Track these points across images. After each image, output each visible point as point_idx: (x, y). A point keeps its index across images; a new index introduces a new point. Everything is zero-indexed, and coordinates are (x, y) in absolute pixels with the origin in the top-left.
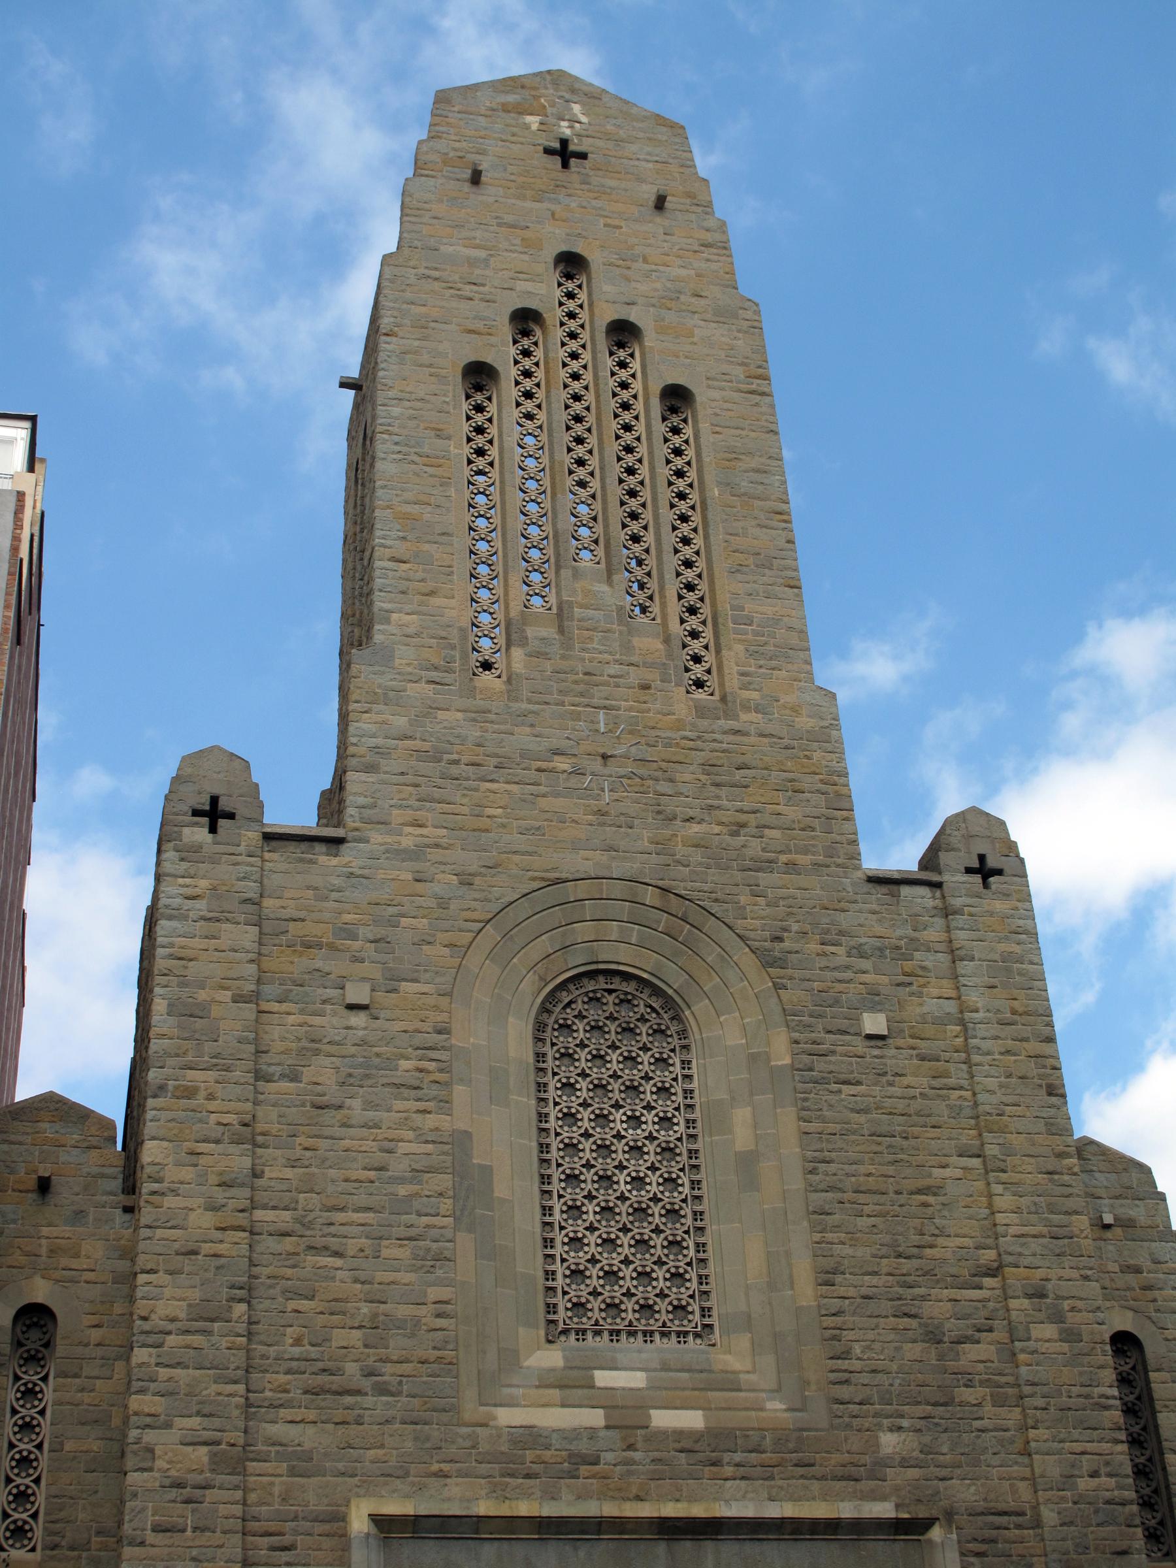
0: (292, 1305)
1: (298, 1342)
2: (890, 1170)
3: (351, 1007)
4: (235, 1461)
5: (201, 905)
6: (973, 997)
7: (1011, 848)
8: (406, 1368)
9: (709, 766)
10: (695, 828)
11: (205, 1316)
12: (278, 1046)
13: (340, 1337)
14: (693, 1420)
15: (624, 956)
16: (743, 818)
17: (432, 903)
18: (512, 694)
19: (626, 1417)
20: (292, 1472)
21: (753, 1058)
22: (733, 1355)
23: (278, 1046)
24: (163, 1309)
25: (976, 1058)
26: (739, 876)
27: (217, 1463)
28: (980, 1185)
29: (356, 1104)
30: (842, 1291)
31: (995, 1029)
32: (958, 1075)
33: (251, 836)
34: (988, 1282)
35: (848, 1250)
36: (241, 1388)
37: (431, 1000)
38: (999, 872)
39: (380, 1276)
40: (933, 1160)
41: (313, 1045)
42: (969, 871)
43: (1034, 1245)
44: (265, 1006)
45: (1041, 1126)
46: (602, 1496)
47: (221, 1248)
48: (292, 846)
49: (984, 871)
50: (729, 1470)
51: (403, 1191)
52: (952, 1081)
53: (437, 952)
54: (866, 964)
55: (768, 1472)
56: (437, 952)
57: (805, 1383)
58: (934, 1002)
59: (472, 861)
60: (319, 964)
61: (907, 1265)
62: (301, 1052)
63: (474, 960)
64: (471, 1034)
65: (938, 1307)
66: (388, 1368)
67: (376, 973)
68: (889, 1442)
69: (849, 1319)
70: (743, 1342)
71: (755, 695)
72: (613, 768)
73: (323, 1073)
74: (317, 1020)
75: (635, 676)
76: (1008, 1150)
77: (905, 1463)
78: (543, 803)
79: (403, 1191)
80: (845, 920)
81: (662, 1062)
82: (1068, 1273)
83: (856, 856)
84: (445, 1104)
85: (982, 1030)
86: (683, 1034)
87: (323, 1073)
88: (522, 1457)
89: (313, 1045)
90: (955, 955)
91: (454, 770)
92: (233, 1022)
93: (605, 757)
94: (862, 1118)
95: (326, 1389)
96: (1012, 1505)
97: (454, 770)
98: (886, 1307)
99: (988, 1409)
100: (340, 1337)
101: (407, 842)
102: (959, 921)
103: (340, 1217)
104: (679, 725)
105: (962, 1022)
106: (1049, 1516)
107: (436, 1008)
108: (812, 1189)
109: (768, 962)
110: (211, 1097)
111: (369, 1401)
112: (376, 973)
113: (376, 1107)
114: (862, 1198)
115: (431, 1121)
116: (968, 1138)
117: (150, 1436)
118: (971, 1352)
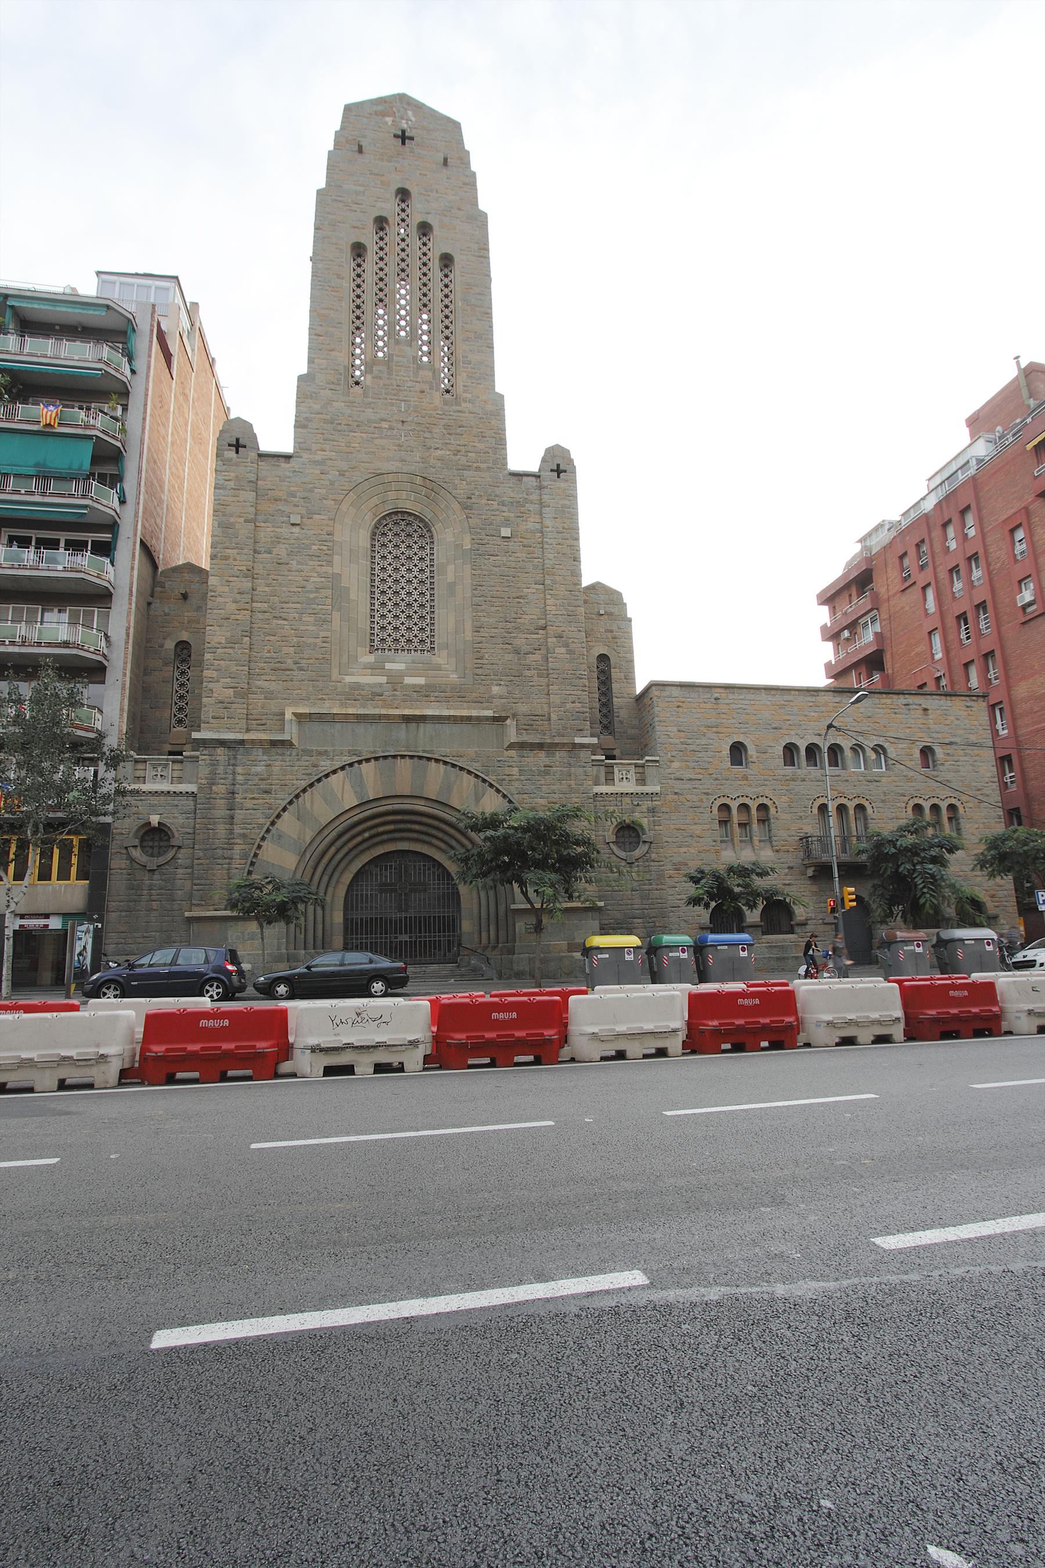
0: (267, 638)
1: (269, 652)
2: (506, 589)
3: (293, 525)
4: (243, 694)
5: (231, 484)
6: (548, 522)
7: (570, 462)
8: (311, 661)
9: (447, 426)
10: (439, 452)
11: (232, 642)
12: (263, 540)
13: (285, 650)
14: (421, 681)
15: (409, 506)
16: (459, 448)
17: (328, 483)
18: (365, 394)
19: (395, 681)
20: (266, 698)
21: (457, 546)
22: (440, 658)
23: (263, 540)
24: (216, 639)
25: (546, 546)
26: (456, 472)
27: (237, 695)
28: (542, 595)
29: (294, 562)
30: (483, 634)
31: (555, 535)
32: (538, 553)
33: (253, 455)
34: (541, 632)
35: (487, 619)
36: (246, 668)
37: (325, 522)
38: (565, 471)
39: (302, 628)
40: (524, 586)
41: (278, 540)
42: (552, 470)
43: (560, 618)
44: (258, 524)
45: (569, 573)
46: (383, 707)
47: (238, 617)
48: (270, 459)
49: (558, 471)
50: (433, 699)
51: (312, 596)
52: (535, 555)
53: (329, 503)
54: (505, 509)
55: (447, 700)
56: (329, 503)
57: (465, 668)
58: (531, 524)
59: (344, 465)
60: (280, 507)
61: (509, 625)
62: (272, 542)
63: (344, 507)
64: (342, 535)
65: (520, 641)
66: (304, 661)
67: (304, 511)
68: (495, 690)
69: (484, 645)
70: (445, 653)
71: (469, 396)
72: (407, 427)
73: (281, 550)
74: (278, 530)
75: (418, 387)
76: (554, 582)
77: (501, 697)
78: (376, 442)
79: (312, 596)
80: (498, 491)
81: (422, 548)
82: (573, 629)
83: (506, 464)
84: (330, 563)
85: (550, 535)
86: (431, 537)
87: (281, 550)
88: (354, 693)
89: (278, 540)
90: (542, 504)
91: (339, 427)
92: (244, 531)
93: (403, 422)
94: (497, 569)
95: (279, 669)
96: (541, 713)
97: (339, 427)
98: (500, 640)
99: (536, 678)
100: (285, 650)
101: (318, 458)
102: (546, 491)
103: (287, 605)
104: (436, 409)
105: (542, 532)
106: (554, 717)
107: (328, 525)
108: (474, 596)
109: (465, 507)
110: (235, 560)
111: (295, 673)
112: (304, 511)
113: (302, 564)
114: (494, 600)
115: (324, 569)
116: (539, 577)
117: (211, 685)
118: (532, 657)
